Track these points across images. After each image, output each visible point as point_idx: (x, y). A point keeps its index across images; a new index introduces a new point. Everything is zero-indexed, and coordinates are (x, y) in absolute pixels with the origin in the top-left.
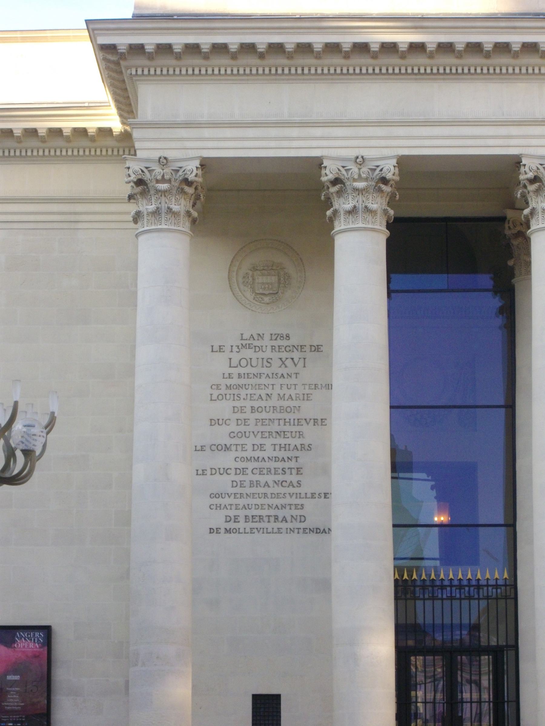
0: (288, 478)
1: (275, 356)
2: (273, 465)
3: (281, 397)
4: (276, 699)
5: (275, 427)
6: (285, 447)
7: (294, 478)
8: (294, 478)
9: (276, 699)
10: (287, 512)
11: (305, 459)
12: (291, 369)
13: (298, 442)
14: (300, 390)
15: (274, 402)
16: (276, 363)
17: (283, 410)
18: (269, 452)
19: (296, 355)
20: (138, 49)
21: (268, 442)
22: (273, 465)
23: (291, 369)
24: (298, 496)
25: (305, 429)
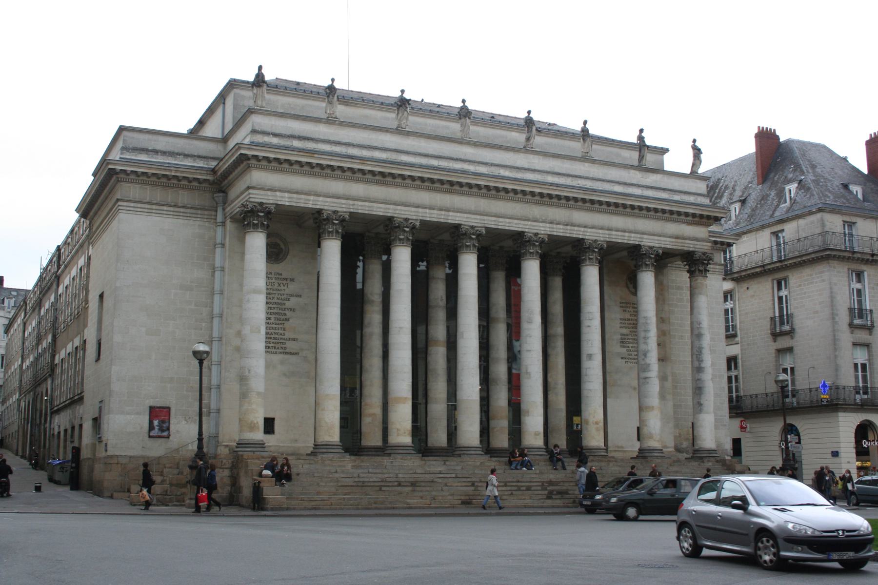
0: (280, 331)
1: (276, 281)
2: (273, 326)
3: (278, 299)
4: (273, 419)
5: (275, 311)
6: (278, 319)
7: (282, 332)
8: (282, 332)
9: (273, 419)
10: (279, 345)
11: (287, 325)
12: (282, 288)
13: (284, 317)
14: (285, 296)
15: (275, 300)
16: (276, 285)
17: (279, 304)
18: (273, 321)
19: (284, 282)
20: (256, 157)
21: (273, 317)
22: (273, 326)
23: (282, 288)
24: (284, 339)
25: (287, 312)
